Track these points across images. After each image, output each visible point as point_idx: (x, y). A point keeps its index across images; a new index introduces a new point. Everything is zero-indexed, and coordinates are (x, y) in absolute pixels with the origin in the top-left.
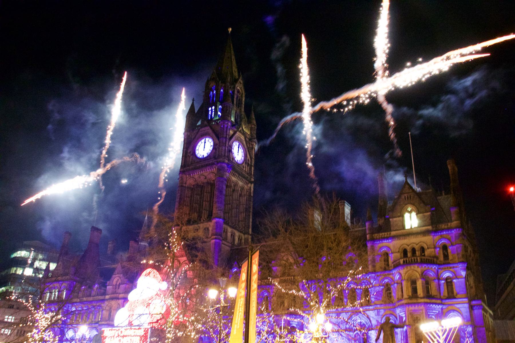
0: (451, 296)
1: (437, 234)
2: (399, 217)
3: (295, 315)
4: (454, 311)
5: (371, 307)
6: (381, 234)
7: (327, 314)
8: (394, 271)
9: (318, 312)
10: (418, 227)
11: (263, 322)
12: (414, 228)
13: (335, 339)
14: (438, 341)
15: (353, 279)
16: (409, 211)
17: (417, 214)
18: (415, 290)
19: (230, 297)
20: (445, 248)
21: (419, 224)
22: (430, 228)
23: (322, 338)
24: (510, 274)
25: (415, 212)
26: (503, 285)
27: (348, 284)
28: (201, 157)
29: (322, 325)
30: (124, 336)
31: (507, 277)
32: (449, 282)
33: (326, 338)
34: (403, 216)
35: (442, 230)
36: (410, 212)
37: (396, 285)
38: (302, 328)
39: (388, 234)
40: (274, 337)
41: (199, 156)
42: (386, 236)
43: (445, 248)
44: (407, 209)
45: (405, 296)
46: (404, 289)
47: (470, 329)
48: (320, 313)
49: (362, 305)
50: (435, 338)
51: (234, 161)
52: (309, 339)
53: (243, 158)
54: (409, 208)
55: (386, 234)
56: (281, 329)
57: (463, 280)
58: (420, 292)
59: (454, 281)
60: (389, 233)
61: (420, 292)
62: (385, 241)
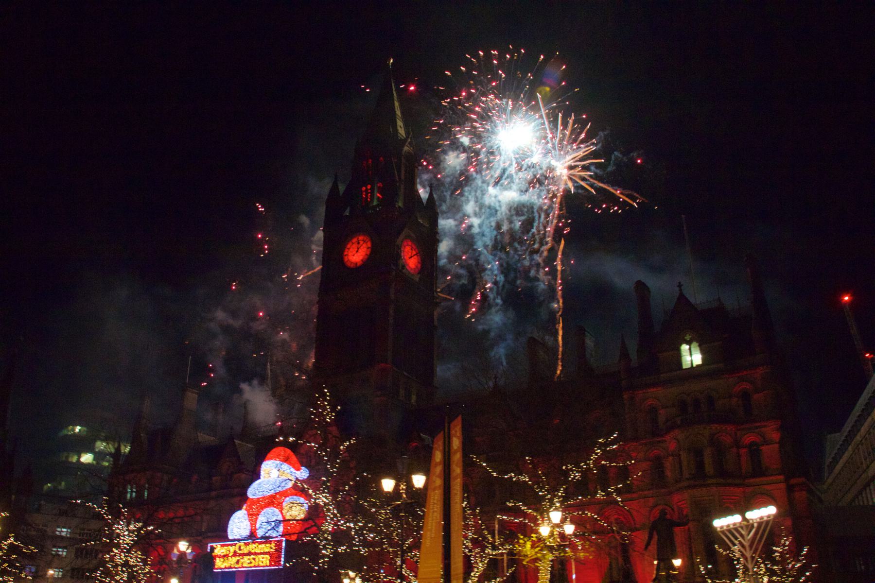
0: (759, 471)
3: (516, 512)
4: (762, 494)
5: (634, 496)
7: (566, 509)
8: (668, 438)
9: (551, 507)
11: (466, 527)
12: (698, 366)
13: (580, 548)
14: (740, 543)
15: (604, 451)
16: (688, 339)
17: (700, 346)
18: (700, 466)
19: (416, 488)
20: (746, 396)
21: (703, 359)
23: (559, 546)
24: (845, 434)
25: (697, 342)
26: (835, 451)
27: (597, 462)
28: (352, 266)
29: (558, 526)
30: (244, 555)
31: (843, 438)
32: (754, 452)
33: (565, 546)
36: (689, 343)
37: (671, 458)
38: (527, 531)
40: (483, 549)
41: (349, 265)
43: (746, 396)
44: (683, 338)
45: (686, 475)
46: (685, 463)
47: (789, 523)
48: (556, 509)
49: (619, 492)
50: (736, 538)
51: (404, 271)
52: (539, 548)
53: (419, 266)
54: (687, 335)
56: (493, 537)
57: (777, 446)
58: (709, 468)
59: (764, 448)
61: (709, 468)
62: (652, 390)
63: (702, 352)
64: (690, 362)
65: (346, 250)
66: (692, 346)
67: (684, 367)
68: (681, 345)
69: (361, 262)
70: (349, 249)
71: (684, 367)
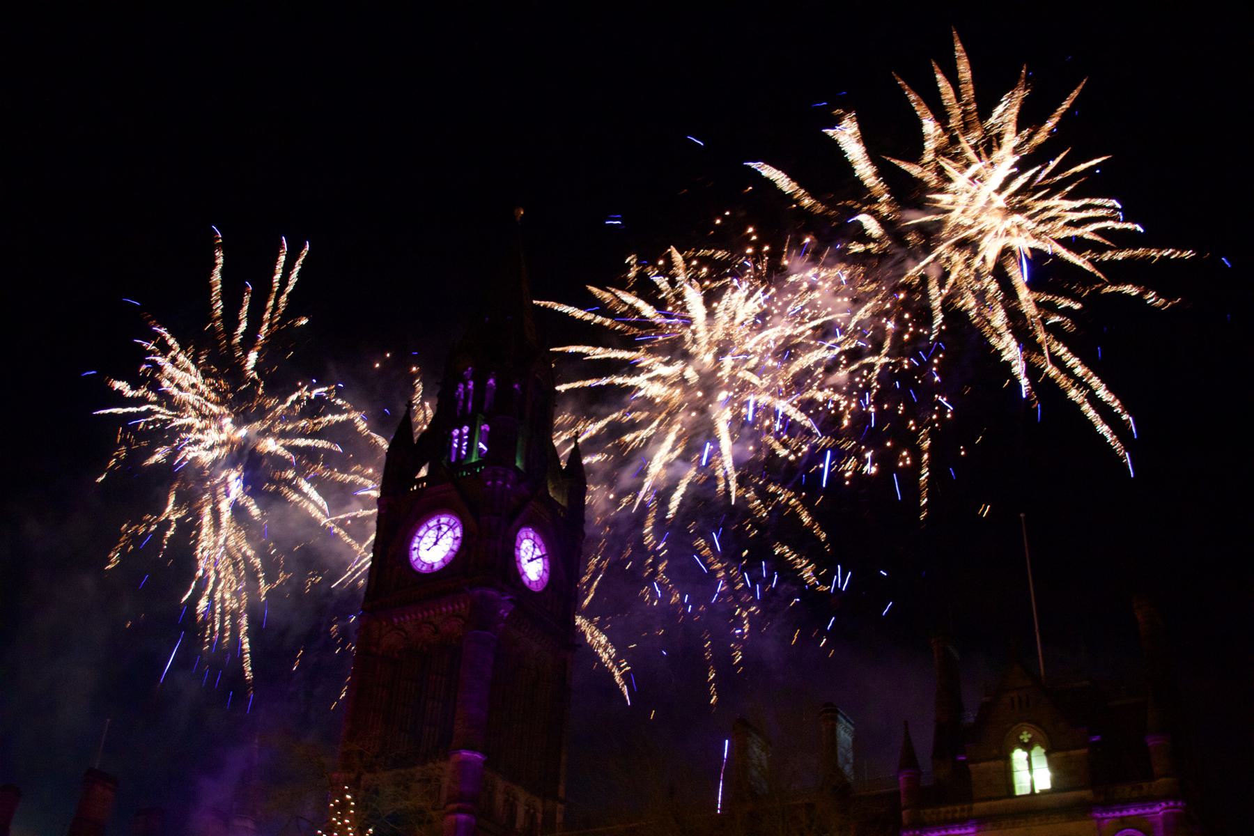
1: (1111, 814)
2: (996, 758)
6: (943, 809)
10: (1054, 790)
12: (1043, 792)
16: (1026, 741)
17: (1047, 754)
22: (1086, 794)
25: (1042, 747)
28: (424, 568)
34: (1008, 760)
35: (1127, 803)
36: (1028, 747)
39: (963, 810)
41: (419, 567)
42: (957, 815)
54: (1025, 733)
55: (958, 808)
60: (966, 807)
63: (1052, 764)
64: (1029, 785)
65: (417, 540)
66: (1033, 753)
67: (1018, 792)
68: (1012, 750)
69: (442, 564)
70: (421, 538)
71: (1018, 792)
